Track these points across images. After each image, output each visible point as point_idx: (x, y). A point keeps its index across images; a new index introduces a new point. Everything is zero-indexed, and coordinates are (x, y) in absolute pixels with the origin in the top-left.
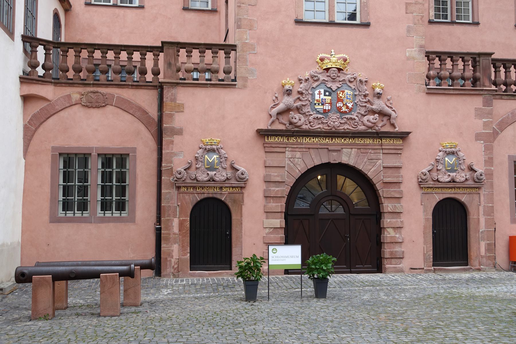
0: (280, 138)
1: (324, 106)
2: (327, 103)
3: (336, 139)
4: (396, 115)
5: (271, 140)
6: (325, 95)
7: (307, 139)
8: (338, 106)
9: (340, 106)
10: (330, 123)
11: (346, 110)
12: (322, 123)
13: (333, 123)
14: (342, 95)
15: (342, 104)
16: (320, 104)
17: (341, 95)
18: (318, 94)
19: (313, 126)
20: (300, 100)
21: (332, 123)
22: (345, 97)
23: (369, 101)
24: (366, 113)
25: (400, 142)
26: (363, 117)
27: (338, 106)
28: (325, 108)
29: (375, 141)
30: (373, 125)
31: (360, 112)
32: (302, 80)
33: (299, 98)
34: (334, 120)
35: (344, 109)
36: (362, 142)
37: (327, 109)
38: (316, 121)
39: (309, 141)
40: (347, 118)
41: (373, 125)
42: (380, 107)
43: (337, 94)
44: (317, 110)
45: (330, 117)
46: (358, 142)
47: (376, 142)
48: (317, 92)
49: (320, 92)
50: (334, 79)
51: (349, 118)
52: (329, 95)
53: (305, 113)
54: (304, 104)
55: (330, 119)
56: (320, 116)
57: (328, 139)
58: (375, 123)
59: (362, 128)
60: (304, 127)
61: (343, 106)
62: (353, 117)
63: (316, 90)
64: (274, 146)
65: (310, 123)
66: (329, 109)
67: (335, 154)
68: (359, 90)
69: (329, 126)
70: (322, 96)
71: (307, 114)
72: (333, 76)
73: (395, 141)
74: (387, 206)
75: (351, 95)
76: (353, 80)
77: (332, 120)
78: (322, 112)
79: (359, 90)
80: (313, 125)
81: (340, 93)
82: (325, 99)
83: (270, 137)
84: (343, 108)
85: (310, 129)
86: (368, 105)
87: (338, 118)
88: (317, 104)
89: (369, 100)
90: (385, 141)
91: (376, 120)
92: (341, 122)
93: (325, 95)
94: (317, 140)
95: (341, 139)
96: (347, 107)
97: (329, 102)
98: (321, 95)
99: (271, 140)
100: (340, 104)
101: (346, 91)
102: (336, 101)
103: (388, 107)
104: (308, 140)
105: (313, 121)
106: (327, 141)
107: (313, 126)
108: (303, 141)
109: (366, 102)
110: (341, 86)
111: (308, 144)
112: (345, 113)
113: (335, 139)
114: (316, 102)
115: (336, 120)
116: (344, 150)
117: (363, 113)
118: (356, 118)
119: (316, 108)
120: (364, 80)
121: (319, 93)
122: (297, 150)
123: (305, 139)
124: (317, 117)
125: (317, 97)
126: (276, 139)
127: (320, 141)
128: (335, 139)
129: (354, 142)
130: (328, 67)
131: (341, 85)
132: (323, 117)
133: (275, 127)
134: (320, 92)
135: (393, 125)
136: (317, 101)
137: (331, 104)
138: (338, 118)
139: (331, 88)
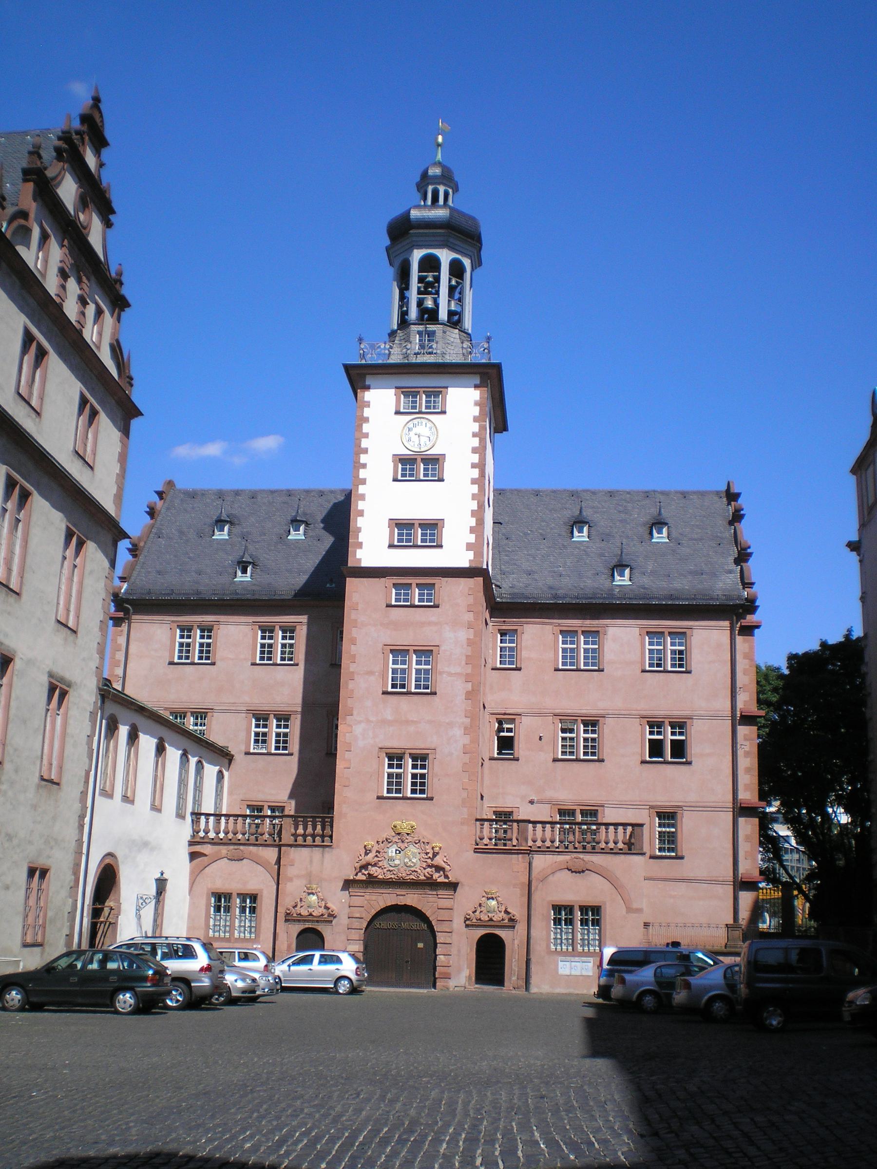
35: (409, 863)
48: (390, 851)
54: (380, 859)
56: (391, 869)
59: (422, 878)
60: (380, 877)
62: (416, 869)
69: (398, 877)
70: (394, 854)
74: (440, 938)
93: (396, 853)
96: (413, 862)
100: (407, 860)
103: (444, 862)
112: (410, 866)
117: (424, 866)
133: (357, 878)
135: (446, 877)
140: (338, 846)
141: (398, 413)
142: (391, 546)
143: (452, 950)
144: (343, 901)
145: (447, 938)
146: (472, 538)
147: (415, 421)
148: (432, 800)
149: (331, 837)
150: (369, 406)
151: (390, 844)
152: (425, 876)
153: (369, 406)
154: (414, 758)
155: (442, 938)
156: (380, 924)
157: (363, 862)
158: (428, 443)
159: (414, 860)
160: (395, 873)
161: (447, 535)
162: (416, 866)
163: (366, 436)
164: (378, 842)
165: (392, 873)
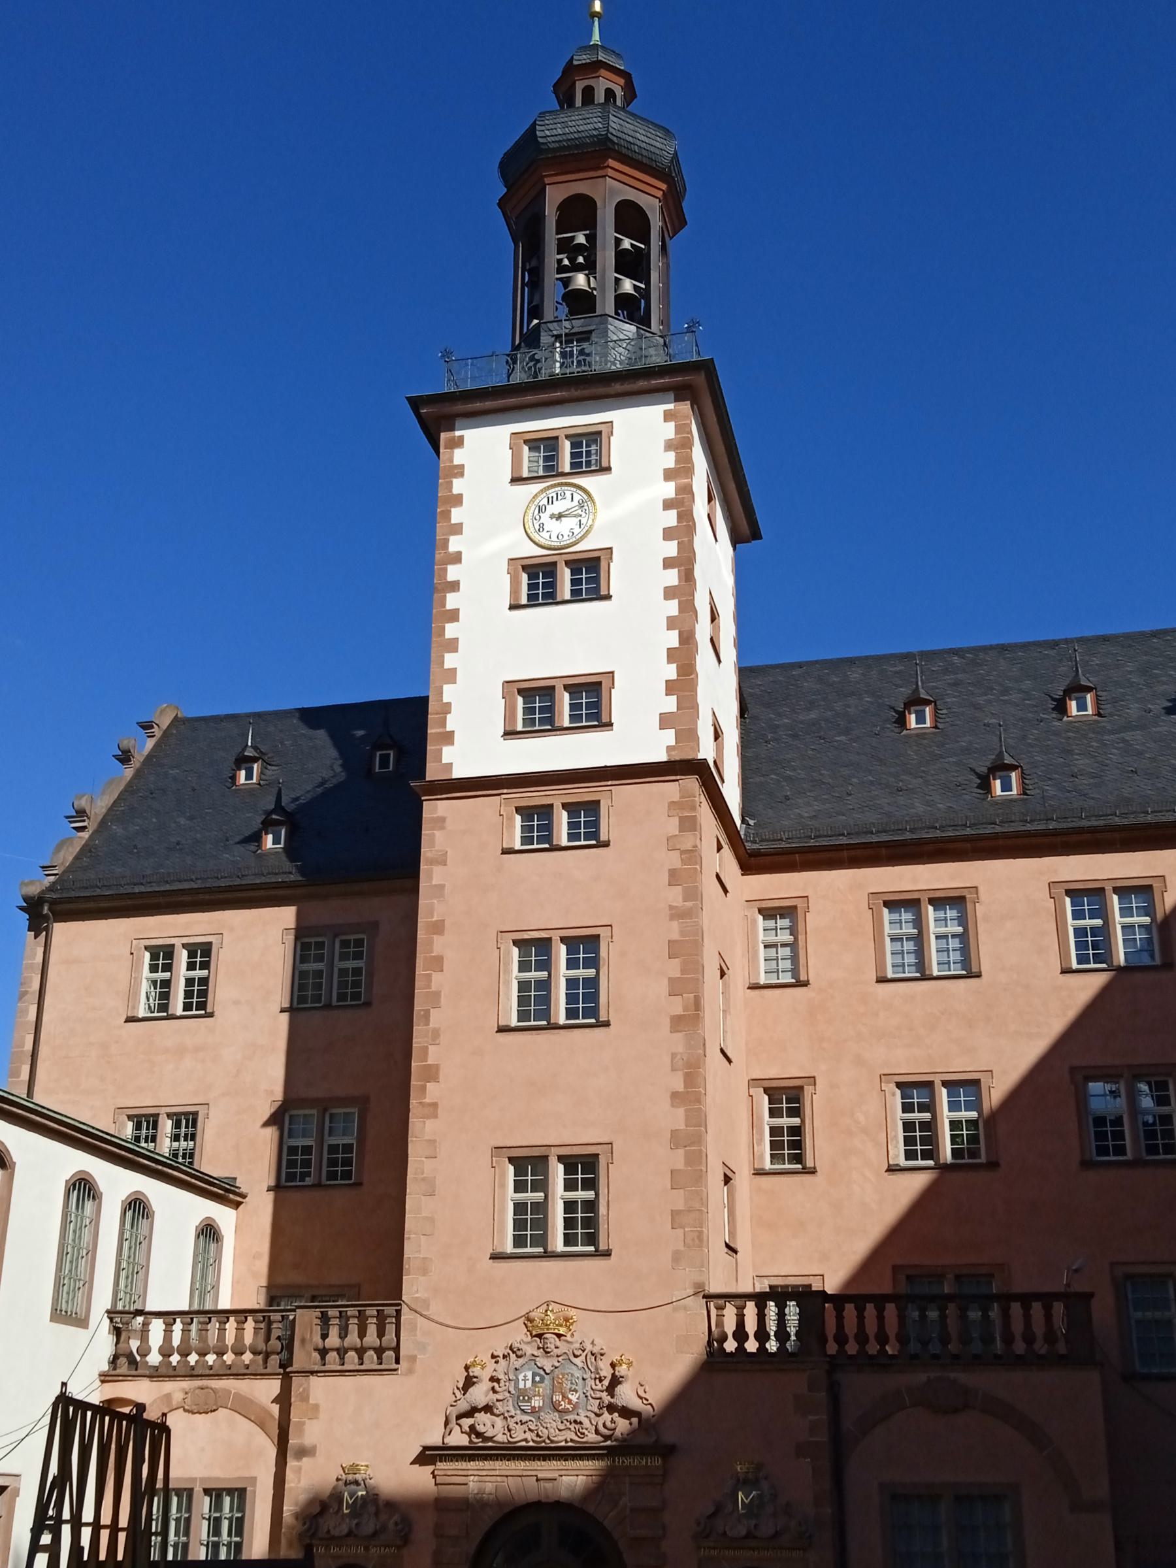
1: (533, 1401)
11: (568, 1406)
19: (513, 1436)
27: (554, 1400)
28: (533, 1405)
30: (611, 1432)
32: (498, 1356)
37: (537, 1405)
41: (611, 1432)
48: (521, 1377)
54: (499, 1397)
56: (525, 1418)
59: (591, 1437)
60: (501, 1438)
62: (578, 1419)
63: (521, 1373)
64: (449, 1473)
66: (541, 1405)
73: (649, 1460)
85: (509, 1442)
96: (570, 1402)
100: (557, 1397)
112: (566, 1411)
119: (520, 1404)
124: (521, 1421)
132: (530, 1421)
134: (525, 1376)
139: (545, 1368)
140: (410, 1371)
141: (516, 480)
142: (509, 734)
146: (670, 704)
147: (552, 493)
148: (610, 1255)
149: (397, 1349)
150: (462, 475)
152: (597, 1432)
153: (462, 475)
154: (570, 1163)
157: (463, 1406)
158: (577, 530)
160: (533, 1427)
161: (620, 703)
163: (458, 529)
164: (493, 1356)
165: (525, 1427)
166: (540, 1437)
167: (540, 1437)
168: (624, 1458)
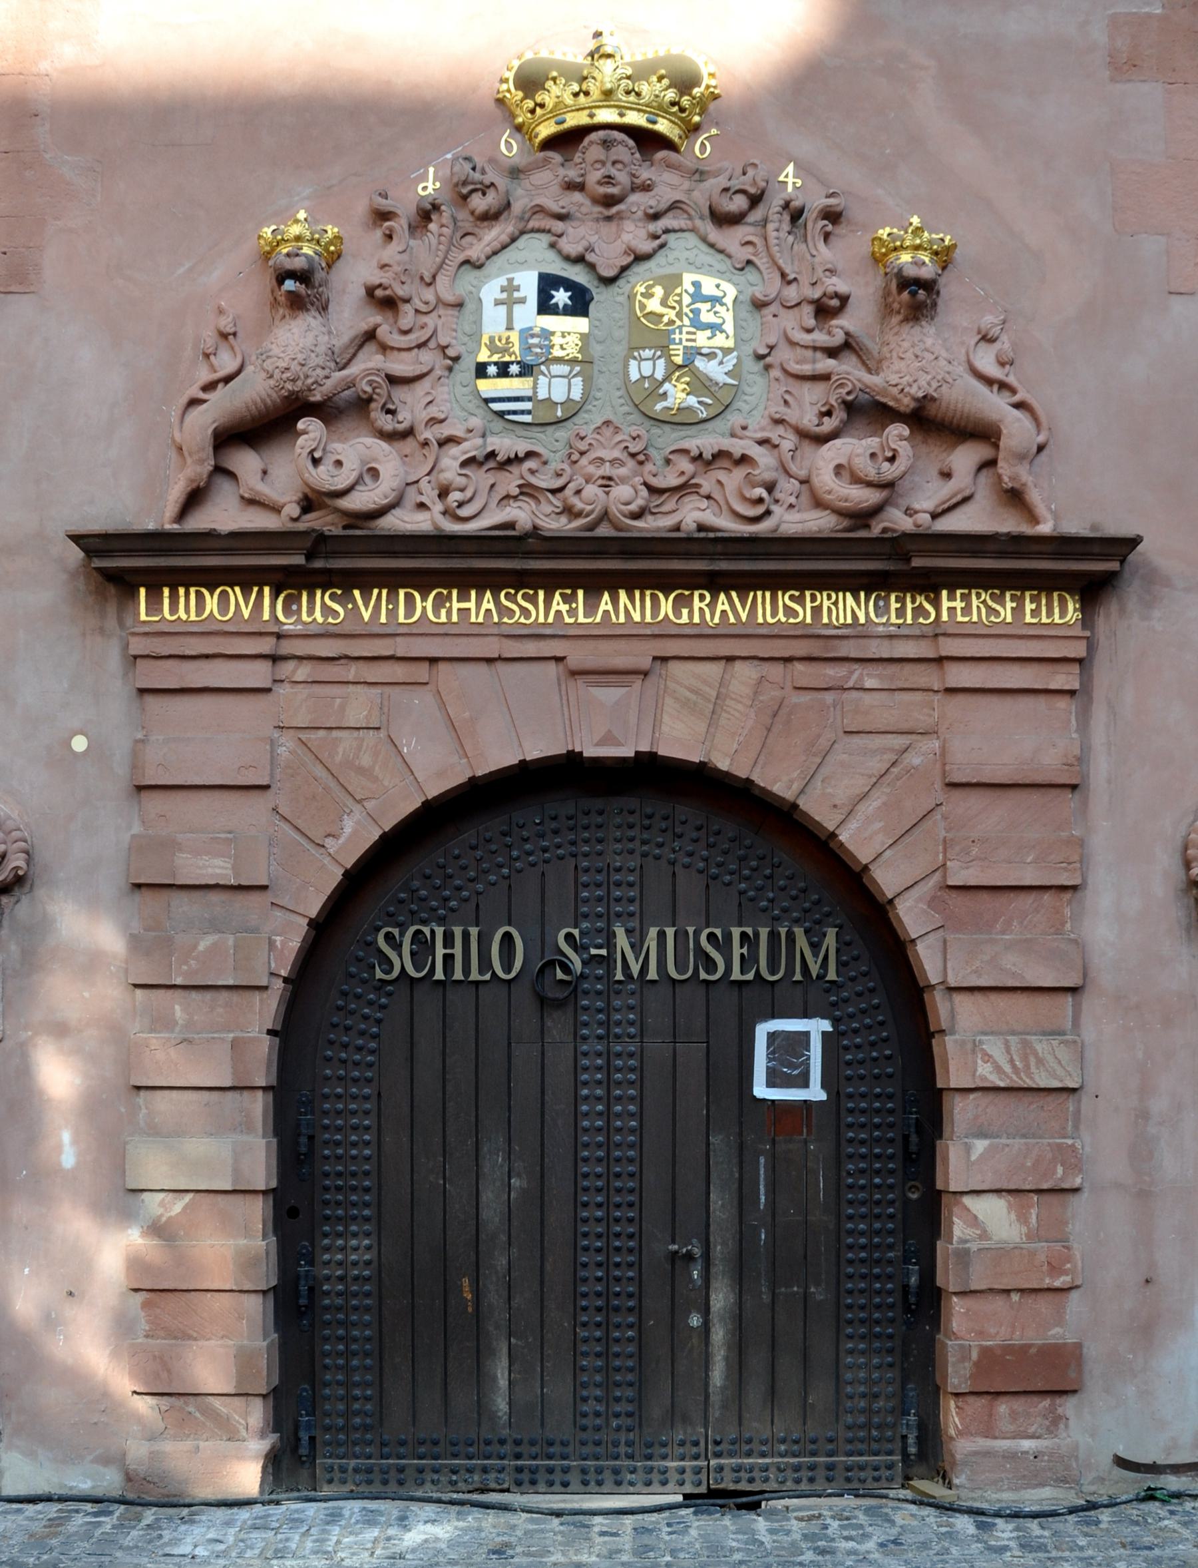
0: (236, 594)
1: (543, 380)
2: (559, 360)
3: (623, 594)
4: (1041, 439)
5: (174, 608)
6: (545, 306)
7: (424, 599)
8: (634, 375)
9: (647, 373)
10: (578, 492)
11: (692, 401)
12: (527, 491)
13: (600, 492)
14: (664, 303)
15: (661, 363)
16: (514, 369)
17: (653, 305)
18: (498, 303)
19: (464, 512)
20: (384, 348)
21: (591, 491)
22: (679, 315)
23: (848, 346)
24: (829, 424)
25: (1063, 614)
26: (807, 448)
27: (634, 375)
28: (542, 394)
29: (894, 605)
30: (870, 497)
31: (792, 415)
33: (370, 336)
34: (607, 470)
35: (677, 394)
36: (804, 614)
37: (559, 395)
38: (481, 478)
39: (437, 615)
40: (695, 452)
42: (923, 379)
43: (631, 297)
44: (496, 406)
45: (582, 453)
46: (774, 613)
47: (901, 613)
49: (510, 288)
50: (609, 201)
51: (707, 455)
52: (580, 304)
53: (409, 433)
54: (401, 366)
55: (584, 461)
56: (506, 444)
57: (566, 599)
58: (889, 485)
61: (667, 378)
62: (738, 447)
63: (489, 278)
65: (443, 493)
66: (576, 394)
67: (608, 695)
68: (783, 275)
69: (569, 511)
70: (527, 314)
71: (427, 434)
72: (600, 183)
73: (1029, 606)
75: (729, 300)
76: (740, 203)
77: (591, 469)
78: (527, 418)
79: (783, 275)
80: (461, 505)
81: (648, 295)
82: (547, 334)
83: (166, 591)
84: (667, 386)
86: (847, 368)
87: (633, 455)
88: (492, 370)
89: (847, 334)
90: (959, 604)
91: (892, 460)
92: (657, 482)
93: (545, 306)
94: (488, 603)
95: (655, 599)
96: (701, 384)
97: (572, 351)
98: (517, 308)
99: (174, 608)
101: (688, 279)
102: (620, 350)
103: (989, 381)
104: (425, 605)
105: (462, 481)
106: (558, 612)
107: (464, 512)
108: (393, 613)
109: (832, 352)
110: (658, 242)
111: (423, 632)
112: (682, 420)
113: (615, 601)
114: (483, 356)
115: (623, 471)
116: (675, 668)
117: (809, 420)
118: (756, 451)
120: (816, 201)
121: (505, 295)
122: (352, 671)
123: (409, 599)
125: (493, 321)
126: (212, 603)
127: (511, 613)
128: (615, 601)
129: (744, 616)
130: (565, 126)
131: (656, 237)
133: (199, 522)
135: (1015, 497)
136: (493, 349)
137: (584, 363)
138: (633, 455)
139: (590, 257)
143: (1085, 1143)
144: (79, 744)
145: (1041, 1046)
151: (494, 234)
155: (994, 1047)
156: (423, 946)
159: (714, 370)
160: (544, 481)
162: (734, 419)
165: (510, 482)
166: (579, 515)
167: (579, 515)
168: (920, 599)
